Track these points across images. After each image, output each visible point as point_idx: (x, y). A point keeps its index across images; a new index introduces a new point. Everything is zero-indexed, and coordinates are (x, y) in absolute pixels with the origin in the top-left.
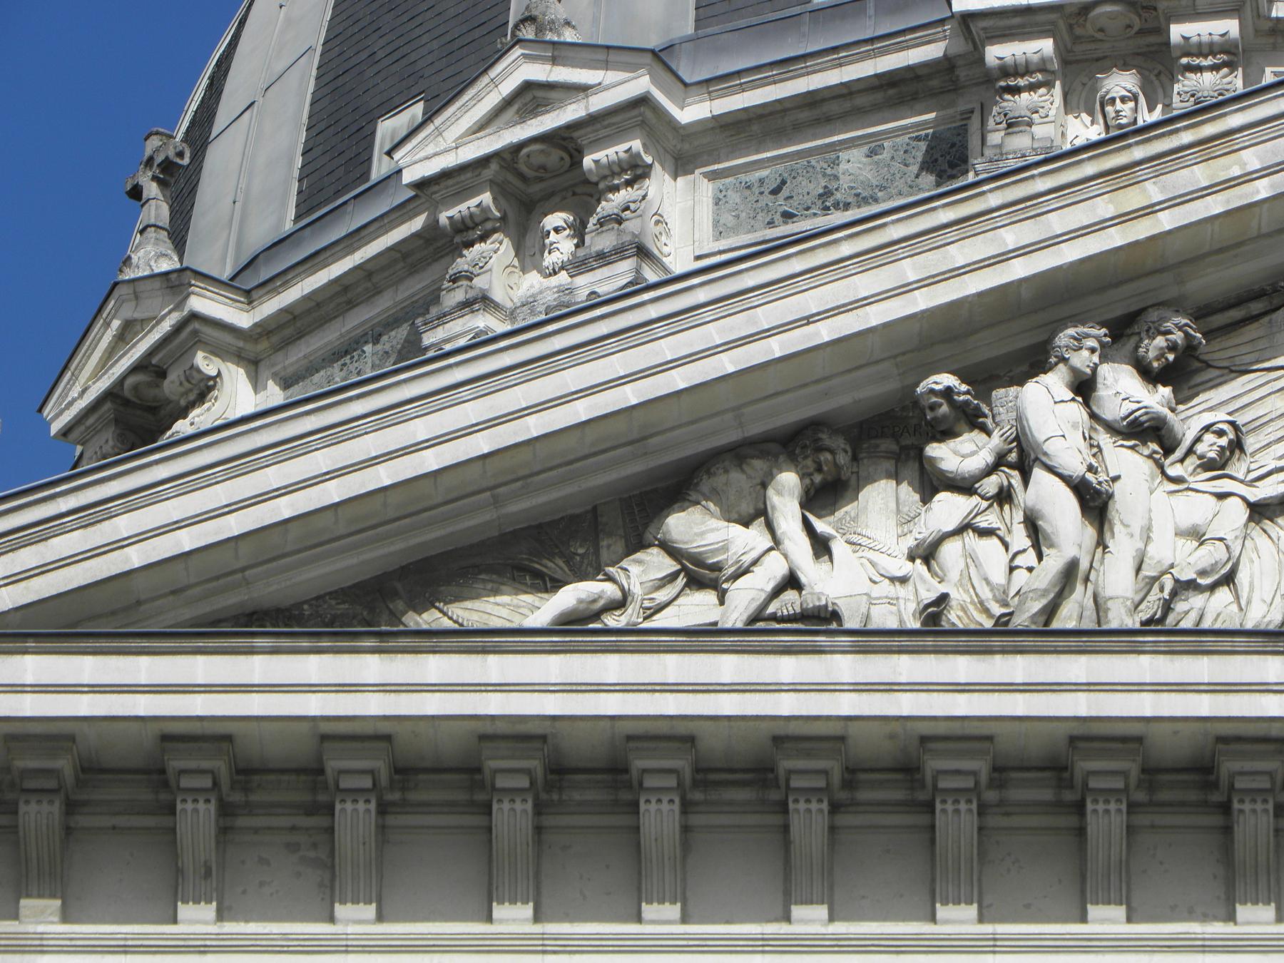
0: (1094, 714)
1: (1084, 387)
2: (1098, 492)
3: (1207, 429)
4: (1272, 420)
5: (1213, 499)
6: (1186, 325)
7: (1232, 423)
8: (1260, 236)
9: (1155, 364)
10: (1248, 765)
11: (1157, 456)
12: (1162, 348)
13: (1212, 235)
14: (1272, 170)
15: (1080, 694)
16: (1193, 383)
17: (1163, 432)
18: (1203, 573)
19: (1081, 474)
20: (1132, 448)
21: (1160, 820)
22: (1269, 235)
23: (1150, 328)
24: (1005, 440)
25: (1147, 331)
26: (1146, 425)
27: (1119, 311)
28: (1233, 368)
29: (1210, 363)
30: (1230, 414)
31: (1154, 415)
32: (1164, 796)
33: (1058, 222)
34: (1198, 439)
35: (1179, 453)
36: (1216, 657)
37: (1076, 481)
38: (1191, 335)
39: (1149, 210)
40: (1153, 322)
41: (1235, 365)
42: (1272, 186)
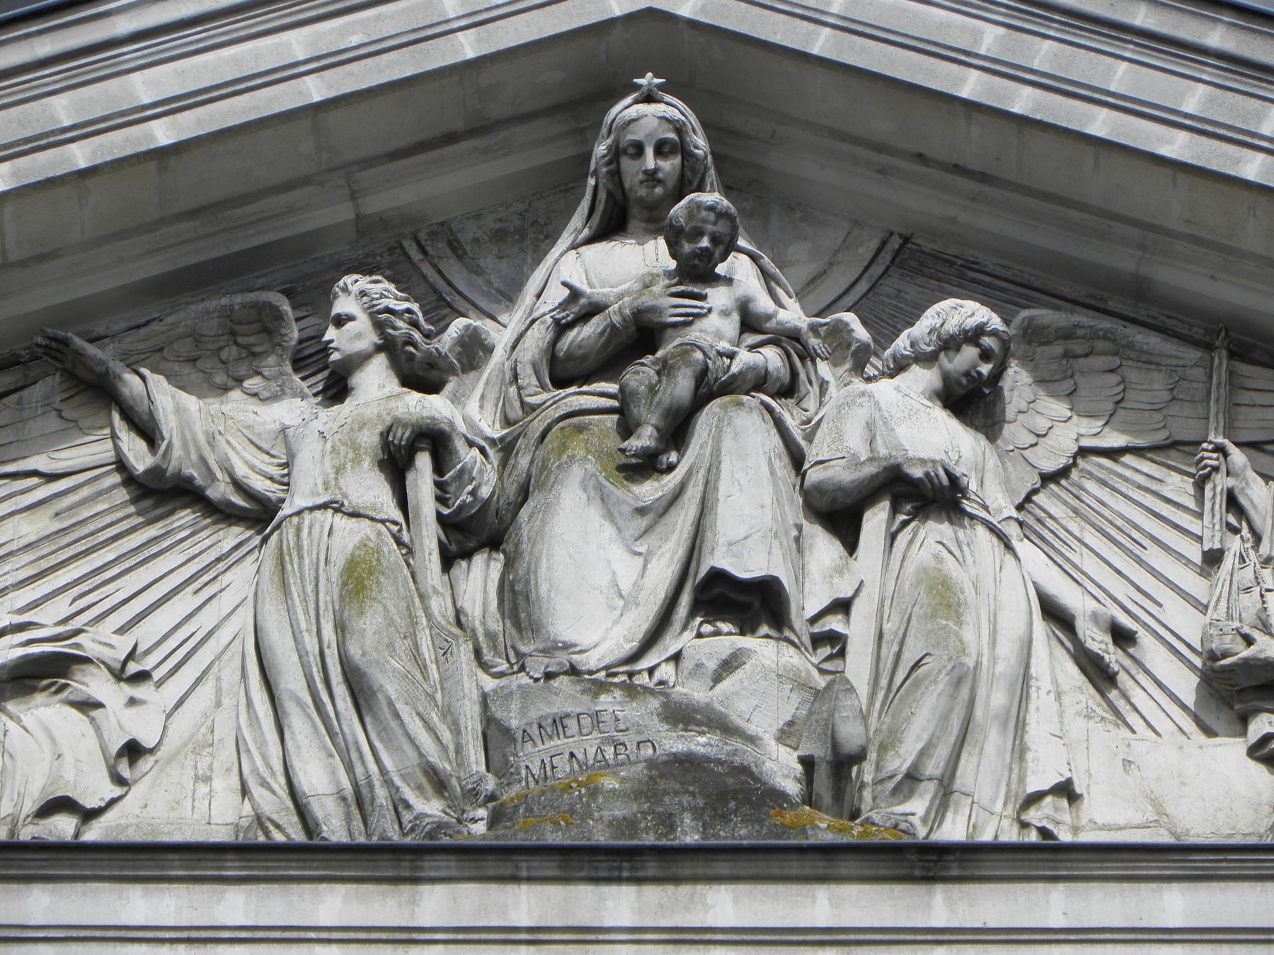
4: (11, 554)
13: (70, 388)
14: (17, 149)
22: (22, 264)
42: (15, 174)
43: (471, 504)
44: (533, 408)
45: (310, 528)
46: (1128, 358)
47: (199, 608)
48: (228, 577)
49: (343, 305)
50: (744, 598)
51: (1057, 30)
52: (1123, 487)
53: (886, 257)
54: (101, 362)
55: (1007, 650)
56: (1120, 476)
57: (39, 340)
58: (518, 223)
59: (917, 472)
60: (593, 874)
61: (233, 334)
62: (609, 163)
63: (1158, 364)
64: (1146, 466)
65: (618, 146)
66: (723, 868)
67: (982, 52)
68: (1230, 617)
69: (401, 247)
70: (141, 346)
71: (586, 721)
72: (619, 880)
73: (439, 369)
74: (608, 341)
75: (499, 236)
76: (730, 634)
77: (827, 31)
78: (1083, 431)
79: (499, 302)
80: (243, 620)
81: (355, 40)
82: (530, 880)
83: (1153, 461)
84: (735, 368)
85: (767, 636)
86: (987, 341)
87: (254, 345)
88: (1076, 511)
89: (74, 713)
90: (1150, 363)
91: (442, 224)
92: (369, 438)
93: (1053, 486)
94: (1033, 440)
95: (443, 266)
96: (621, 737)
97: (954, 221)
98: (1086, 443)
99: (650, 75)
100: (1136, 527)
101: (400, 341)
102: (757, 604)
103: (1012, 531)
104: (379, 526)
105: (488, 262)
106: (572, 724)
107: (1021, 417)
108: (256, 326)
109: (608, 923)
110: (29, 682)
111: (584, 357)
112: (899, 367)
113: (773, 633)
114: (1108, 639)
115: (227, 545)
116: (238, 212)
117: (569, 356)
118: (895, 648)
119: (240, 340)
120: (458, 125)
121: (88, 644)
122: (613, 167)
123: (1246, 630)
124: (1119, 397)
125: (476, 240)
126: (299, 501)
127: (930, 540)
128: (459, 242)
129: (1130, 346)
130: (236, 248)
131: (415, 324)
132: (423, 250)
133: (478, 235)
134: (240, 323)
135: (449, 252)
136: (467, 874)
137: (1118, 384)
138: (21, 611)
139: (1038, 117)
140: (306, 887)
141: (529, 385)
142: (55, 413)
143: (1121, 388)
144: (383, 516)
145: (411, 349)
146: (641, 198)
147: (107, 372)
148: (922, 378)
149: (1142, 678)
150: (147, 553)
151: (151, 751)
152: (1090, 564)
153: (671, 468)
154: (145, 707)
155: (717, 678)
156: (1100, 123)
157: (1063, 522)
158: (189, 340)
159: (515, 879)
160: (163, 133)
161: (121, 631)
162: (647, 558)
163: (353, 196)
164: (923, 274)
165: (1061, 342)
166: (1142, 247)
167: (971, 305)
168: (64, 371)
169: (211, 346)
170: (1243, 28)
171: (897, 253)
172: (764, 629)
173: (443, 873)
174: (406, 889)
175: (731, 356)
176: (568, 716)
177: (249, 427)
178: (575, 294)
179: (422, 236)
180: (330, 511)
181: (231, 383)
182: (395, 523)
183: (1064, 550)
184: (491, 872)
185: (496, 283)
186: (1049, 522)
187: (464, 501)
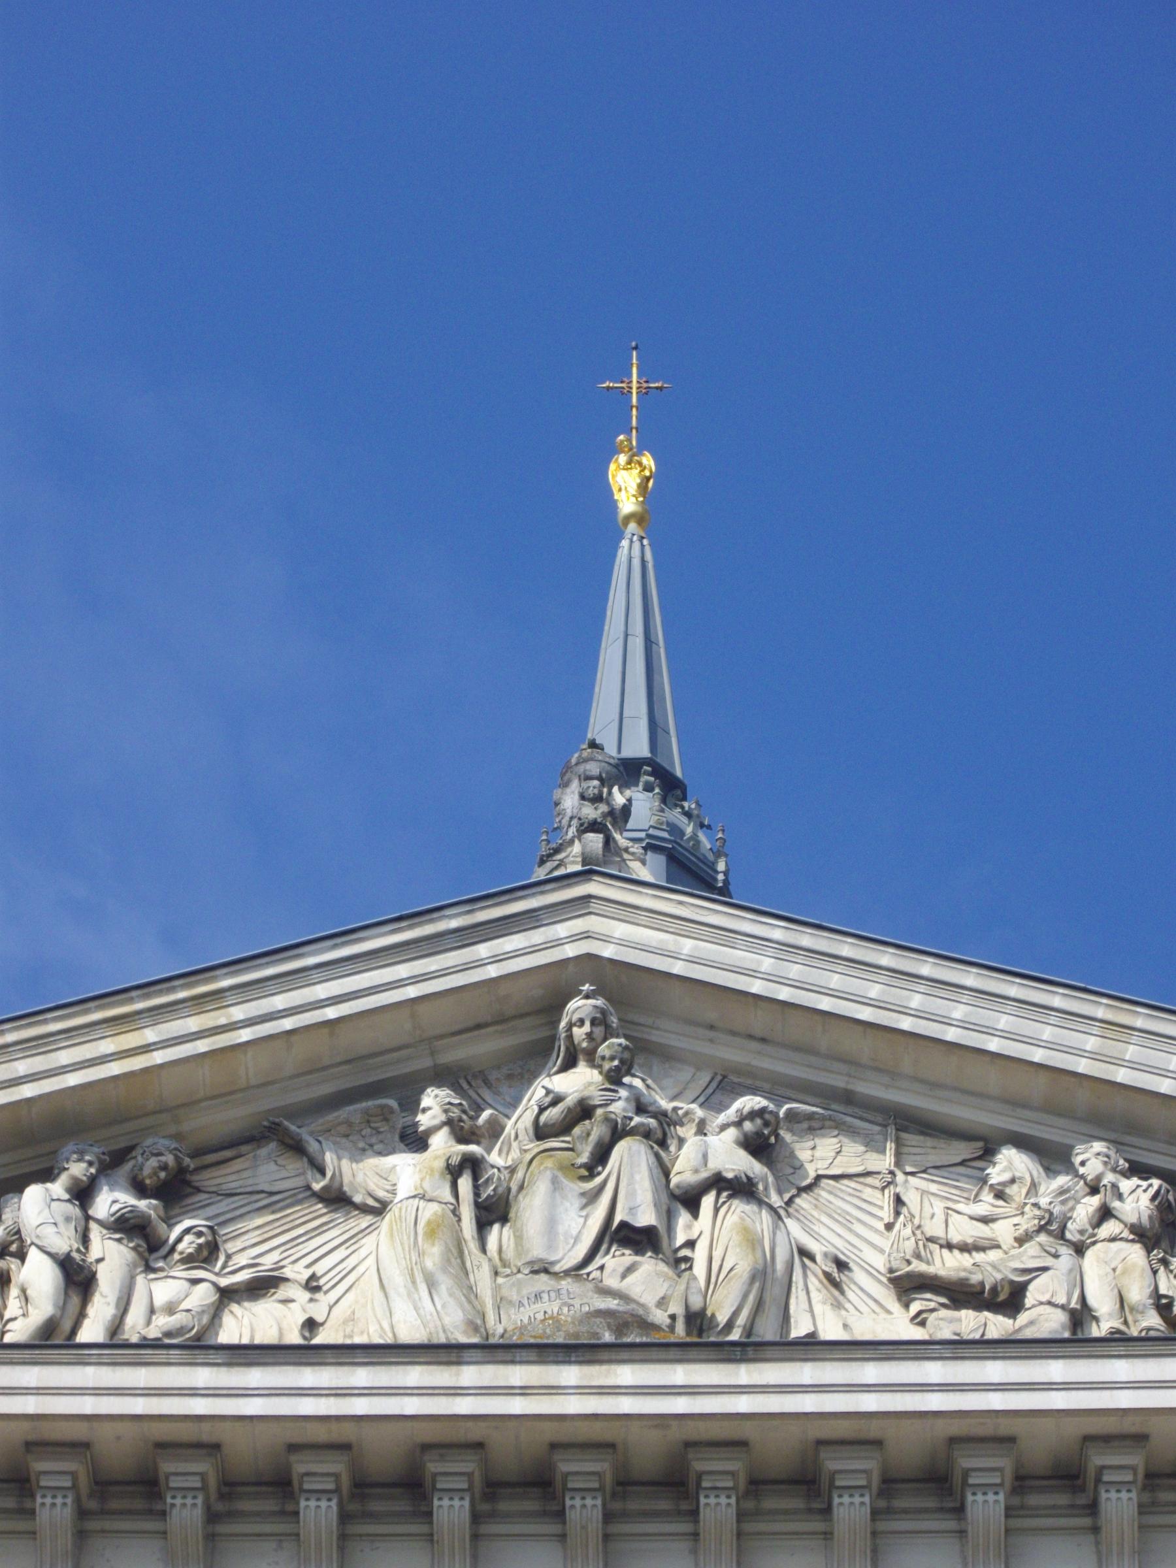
0: (40, 1411)
1: (82, 1194)
2: (81, 1267)
3: (187, 1231)
5: (186, 1284)
6: (176, 1149)
7: (210, 1228)
8: (249, 1088)
9: (148, 1181)
10: (182, 1467)
11: (141, 1249)
12: (154, 1168)
15: (30, 1397)
16: (184, 1203)
17: (148, 1230)
18: (168, 1334)
19: (66, 1251)
20: (119, 1240)
21: (108, 1524)
23: (145, 1151)
24: (8, 1233)
25: (142, 1154)
26: (132, 1221)
27: (122, 1144)
28: (220, 1192)
29: (202, 1188)
30: (207, 1219)
31: (140, 1214)
32: (114, 1505)
33: (64, 1057)
34: (179, 1240)
35: (164, 1251)
36: (152, 1369)
37: (62, 1258)
38: (179, 1157)
39: (146, 1049)
40: (148, 1147)
41: (221, 1190)
43: (493, 1196)
44: (526, 1151)
45: (406, 1208)
46: (843, 1130)
47: (347, 1257)
48: (364, 1241)
49: (424, 1103)
50: (638, 1237)
51: (802, 959)
52: (842, 1195)
53: (714, 1085)
54: (298, 1134)
55: (780, 1266)
56: (840, 1189)
57: (266, 1123)
58: (520, 1071)
59: (730, 1175)
60: (556, 1359)
61: (368, 1122)
62: (567, 1031)
63: (858, 1133)
64: (853, 1184)
65: (571, 1023)
66: (625, 1355)
67: (763, 970)
68: (898, 1251)
69: (458, 1083)
70: (319, 1128)
71: (553, 1294)
72: (569, 1362)
73: (477, 1136)
74: (566, 1116)
75: (510, 1077)
76: (630, 1255)
77: (681, 962)
78: (819, 1166)
79: (509, 1108)
80: (371, 1261)
81: (433, 968)
82: (521, 1362)
83: (857, 1182)
84: (633, 1124)
85: (651, 1257)
86: (767, 1116)
87: (379, 1128)
88: (816, 1206)
89: (280, 1306)
90: (854, 1132)
91: (480, 1072)
92: (440, 1164)
93: (804, 1195)
94: (792, 1171)
95: (480, 1091)
96: (571, 1301)
97: (749, 1065)
98: (820, 1172)
99: (587, 985)
100: (848, 1213)
101: (456, 1119)
102: (646, 1241)
103: (782, 1213)
104: (444, 1206)
105: (504, 1089)
106: (545, 1296)
107: (786, 1160)
108: (382, 1117)
109: (563, 1384)
110: (257, 1292)
111: (553, 1125)
112: (723, 1128)
113: (653, 1255)
114: (834, 1266)
115: (364, 1225)
116: (370, 1061)
117: (545, 1125)
118: (719, 1263)
119: (372, 1125)
120: (489, 1019)
121: (288, 1272)
122: (569, 1033)
123: (908, 1257)
124: (839, 1149)
125: (497, 1079)
126: (402, 1193)
127: (738, 1210)
128: (488, 1080)
129: (844, 1123)
130: (370, 1080)
131: (464, 1112)
132: (469, 1083)
133: (499, 1076)
134: (372, 1116)
135: (483, 1084)
136: (486, 1359)
137: (838, 1143)
138: (254, 1258)
139: (792, 1001)
140: (400, 1368)
141: (524, 1140)
142: (273, 1163)
143: (839, 1145)
144: (445, 1201)
145: (462, 1124)
146: (584, 1048)
147: (301, 1140)
148: (732, 1132)
149: (852, 1286)
150: (321, 1230)
151: (322, 1324)
152: (824, 1232)
153: (599, 1174)
154: (318, 1303)
155: (624, 1276)
156: (825, 1004)
157: (810, 1211)
158: (345, 1125)
159: (513, 1362)
160: (331, 1013)
161: (308, 1266)
162: (586, 1217)
163: (432, 1053)
164: (733, 1092)
165: (807, 1122)
166: (849, 1076)
167: (758, 1099)
168: (279, 1140)
169: (357, 1128)
170: (900, 955)
171: (721, 1082)
172: (649, 1254)
173: (474, 1359)
174: (454, 1368)
175: (631, 1119)
176: (543, 1292)
177: (376, 1166)
178: (548, 1092)
179: (469, 1078)
180: (417, 1200)
181: (367, 1147)
182: (452, 1204)
183: (810, 1224)
184: (500, 1359)
185: (508, 1099)
186: (802, 1212)
187: (489, 1195)
